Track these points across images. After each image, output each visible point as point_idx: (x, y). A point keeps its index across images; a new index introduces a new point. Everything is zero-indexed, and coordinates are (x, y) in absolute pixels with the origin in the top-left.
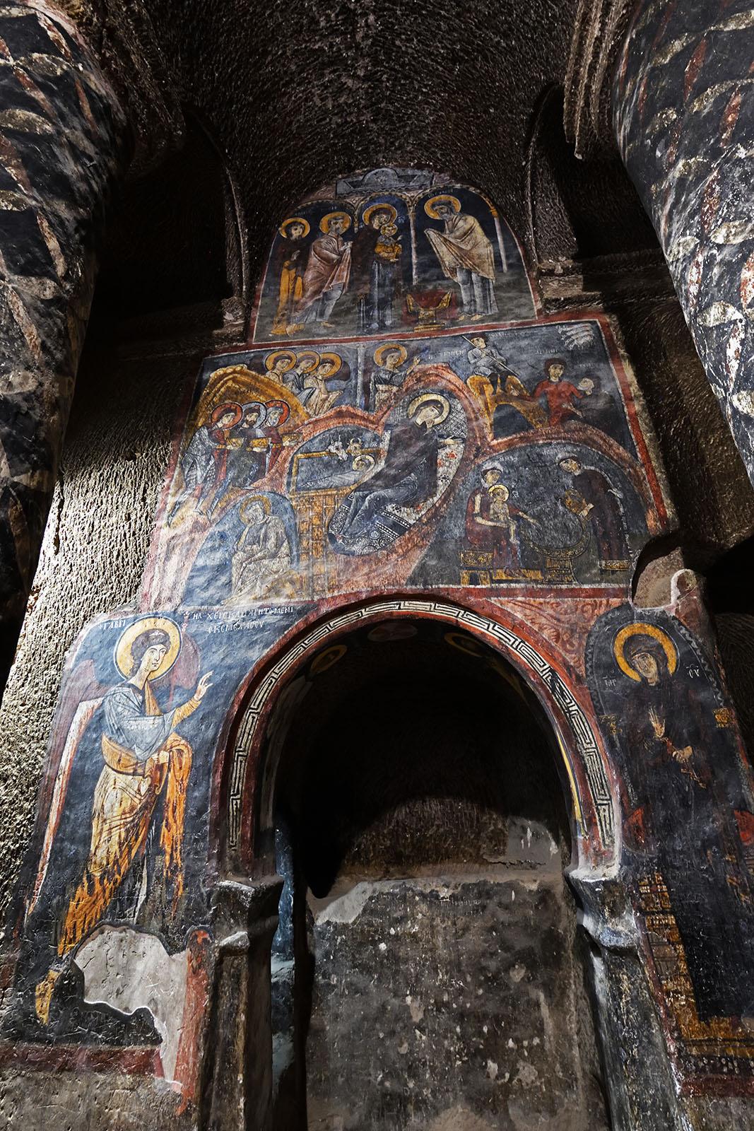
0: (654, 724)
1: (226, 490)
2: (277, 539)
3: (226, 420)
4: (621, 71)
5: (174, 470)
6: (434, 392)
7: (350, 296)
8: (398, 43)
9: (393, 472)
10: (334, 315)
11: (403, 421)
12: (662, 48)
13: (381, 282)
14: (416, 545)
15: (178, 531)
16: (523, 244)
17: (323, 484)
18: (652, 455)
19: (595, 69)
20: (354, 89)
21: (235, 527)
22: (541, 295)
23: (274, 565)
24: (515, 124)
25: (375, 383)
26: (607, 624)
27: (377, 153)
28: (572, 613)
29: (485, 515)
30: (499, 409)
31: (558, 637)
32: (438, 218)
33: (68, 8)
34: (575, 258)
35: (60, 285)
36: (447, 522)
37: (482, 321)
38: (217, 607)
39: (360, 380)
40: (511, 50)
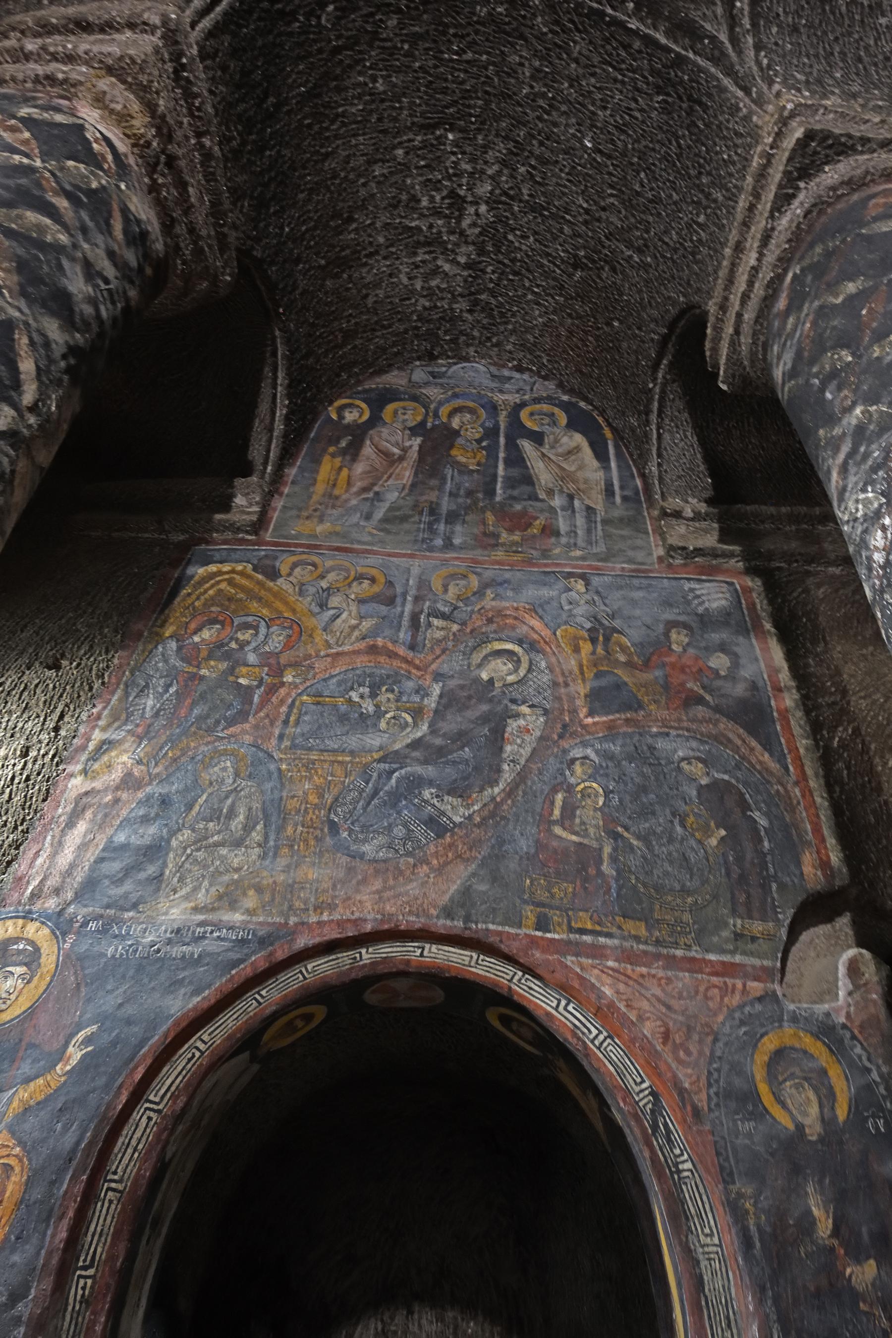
0: (815, 1212)
1: (185, 733)
2: (247, 818)
3: (206, 634)
4: (782, 303)
5: (113, 693)
6: (509, 640)
7: (410, 501)
8: (510, 237)
9: (438, 741)
10: (385, 520)
11: (461, 673)
12: (832, 287)
14: (460, 856)
15: (97, 784)
16: (643, 476)
17: (332, 744)
18: (809, 772)
19: (749, 297)
20: (451, 274)
21: (187, 789)
22: (664, 540)
23: (236, 858)
24: (643, 342)
25: (429, 615)
26: (742, 1023)
27: (468, 345)
28: (691, 998)
29: (567, 823)
30: (598, 675)
31: (666, 1036)
32: (536, 429)
33: (125, 127)
34: (709, 502)
35: (21, 416)
36: (511, 827)
37: (583, 558)
38: (131, 914)
39: (408, 608)
40: (645, 266)
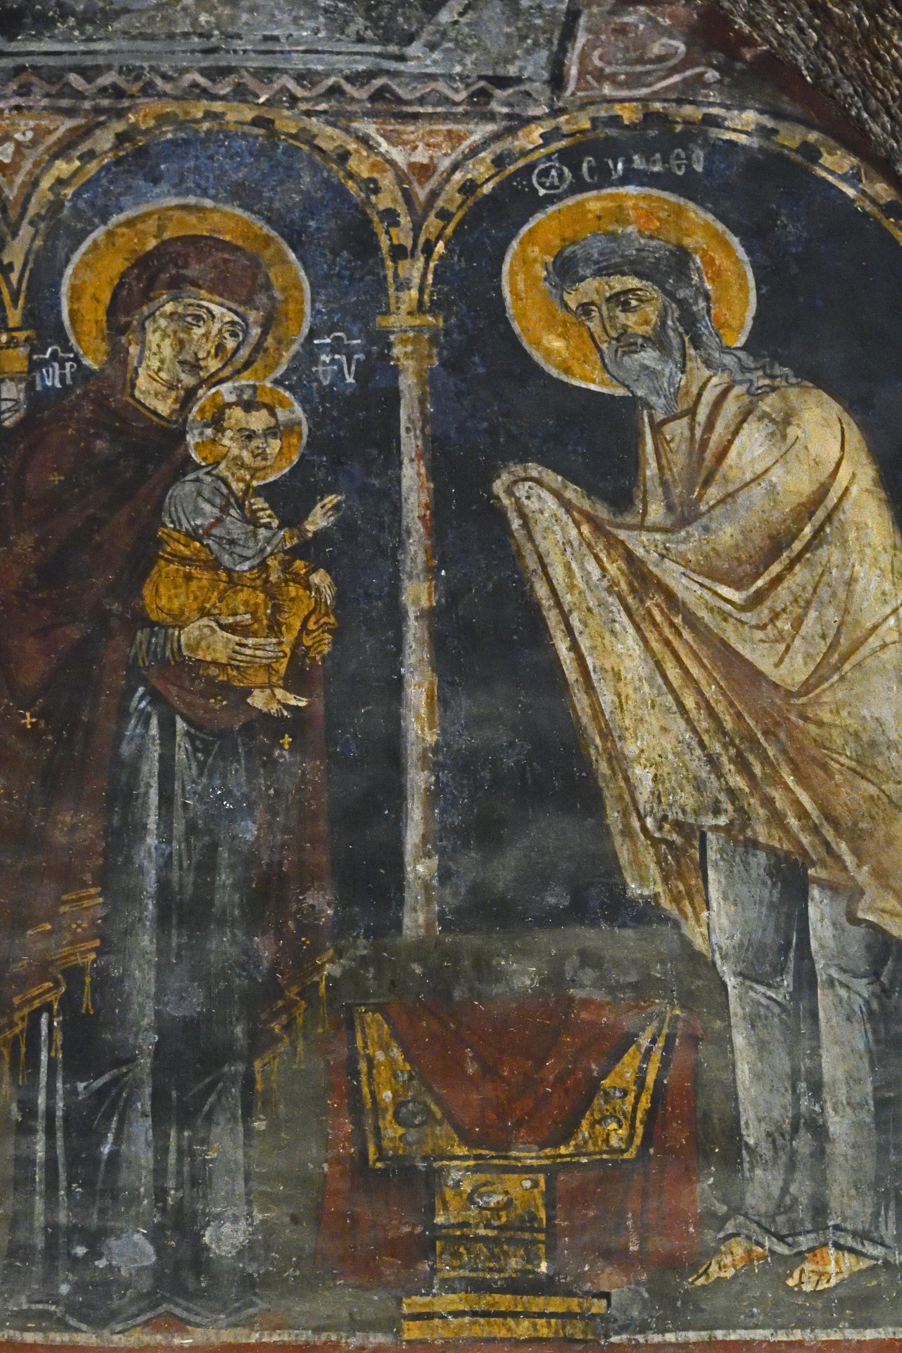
13: (184, 879)
